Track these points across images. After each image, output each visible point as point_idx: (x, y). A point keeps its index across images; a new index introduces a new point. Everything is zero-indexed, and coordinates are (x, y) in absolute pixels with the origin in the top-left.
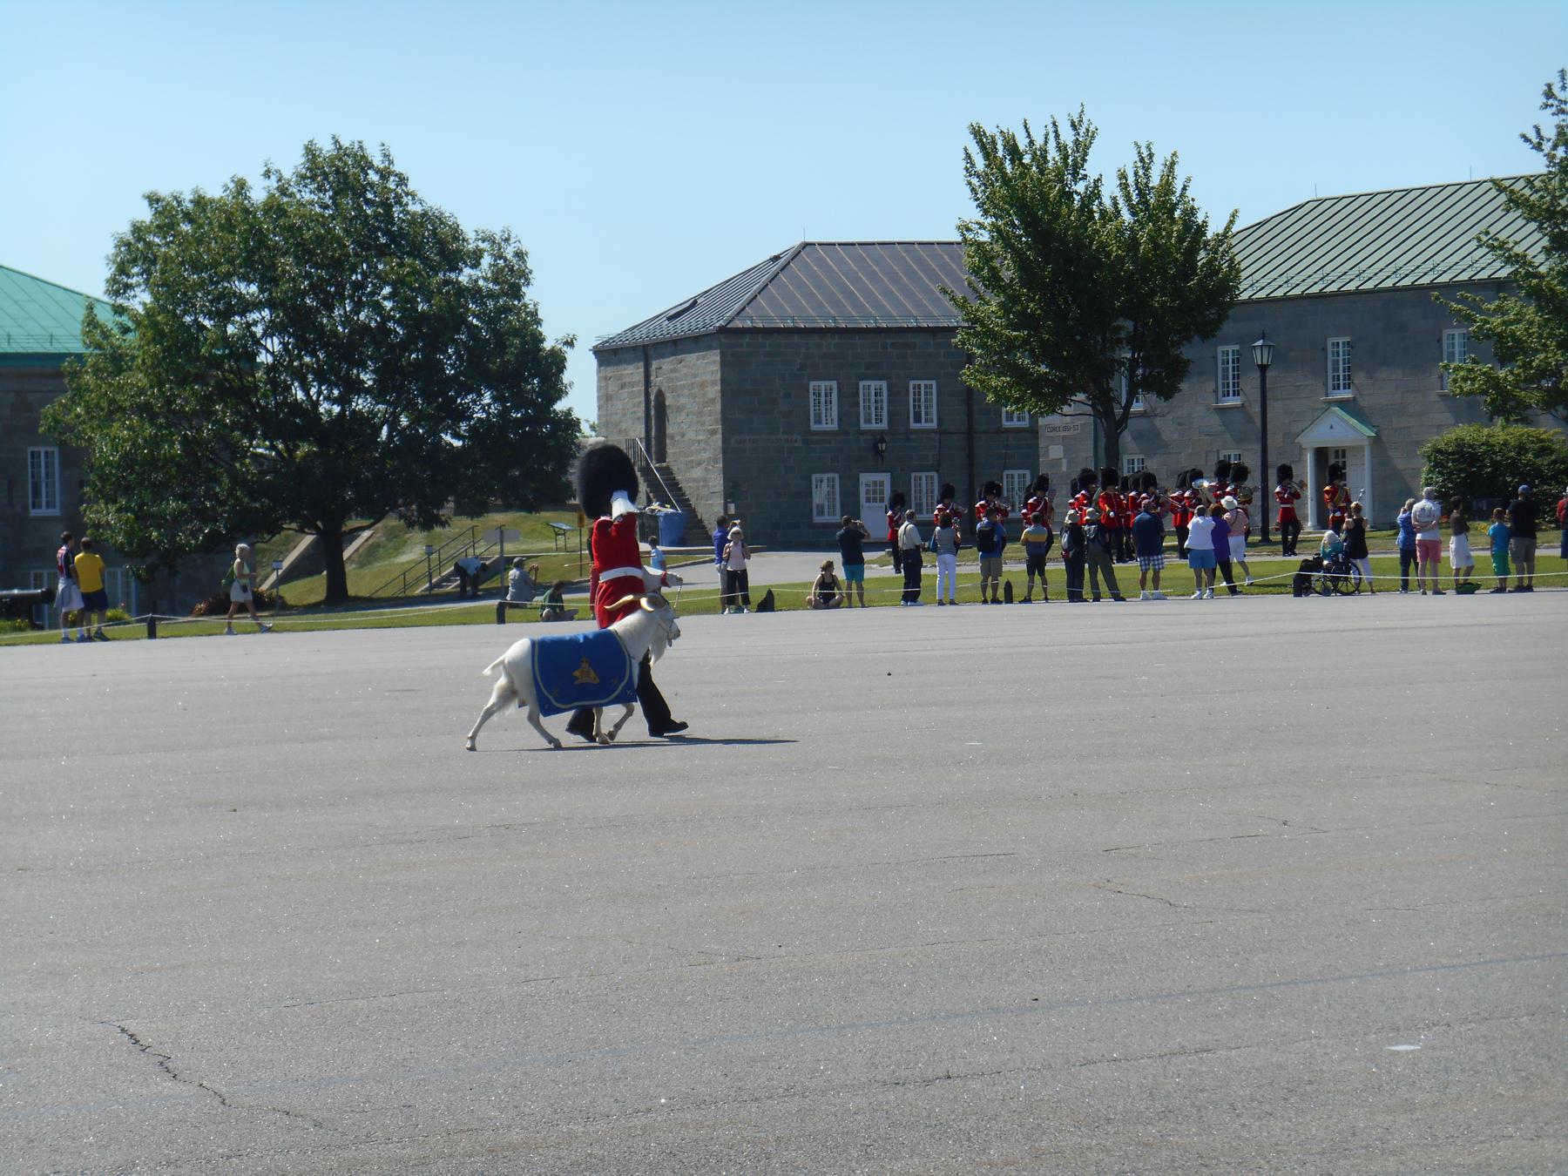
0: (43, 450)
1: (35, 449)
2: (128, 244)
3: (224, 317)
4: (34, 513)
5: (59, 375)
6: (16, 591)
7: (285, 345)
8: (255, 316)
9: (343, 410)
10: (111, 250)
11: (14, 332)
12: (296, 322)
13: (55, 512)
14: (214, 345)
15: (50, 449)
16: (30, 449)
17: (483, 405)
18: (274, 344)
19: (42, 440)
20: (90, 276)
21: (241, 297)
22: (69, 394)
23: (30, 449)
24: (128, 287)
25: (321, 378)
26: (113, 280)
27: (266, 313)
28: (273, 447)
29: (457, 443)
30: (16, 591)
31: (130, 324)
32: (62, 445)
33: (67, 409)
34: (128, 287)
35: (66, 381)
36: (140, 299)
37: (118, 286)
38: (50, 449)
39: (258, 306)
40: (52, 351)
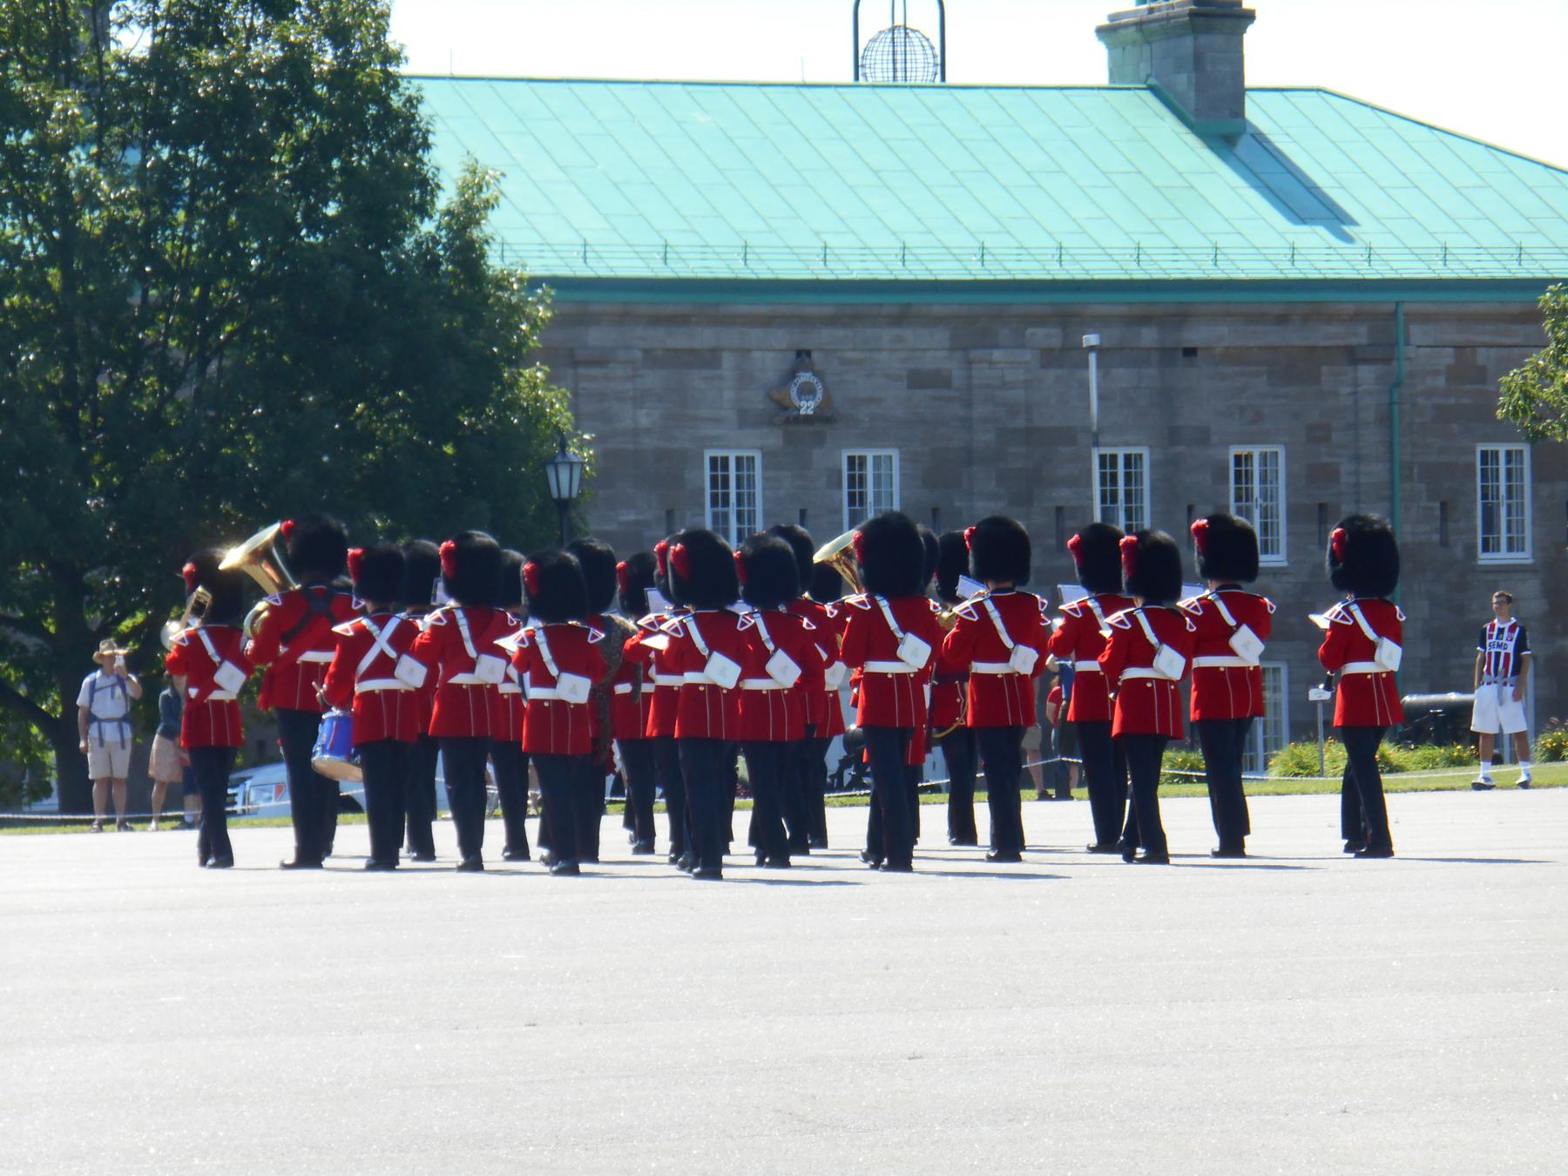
0: (1502, 449)
1: (1489, 447)
5: (1534, 317)
11: (1454, 241)
13: (1524, 557)
15: (1514, 447)
19: (1503, 432)
22: (1552, 349)
32: (1536, 438)
33: (1545, 377)
35: (1547, 325)
38: (1514, 447)
40: (1522, 274)
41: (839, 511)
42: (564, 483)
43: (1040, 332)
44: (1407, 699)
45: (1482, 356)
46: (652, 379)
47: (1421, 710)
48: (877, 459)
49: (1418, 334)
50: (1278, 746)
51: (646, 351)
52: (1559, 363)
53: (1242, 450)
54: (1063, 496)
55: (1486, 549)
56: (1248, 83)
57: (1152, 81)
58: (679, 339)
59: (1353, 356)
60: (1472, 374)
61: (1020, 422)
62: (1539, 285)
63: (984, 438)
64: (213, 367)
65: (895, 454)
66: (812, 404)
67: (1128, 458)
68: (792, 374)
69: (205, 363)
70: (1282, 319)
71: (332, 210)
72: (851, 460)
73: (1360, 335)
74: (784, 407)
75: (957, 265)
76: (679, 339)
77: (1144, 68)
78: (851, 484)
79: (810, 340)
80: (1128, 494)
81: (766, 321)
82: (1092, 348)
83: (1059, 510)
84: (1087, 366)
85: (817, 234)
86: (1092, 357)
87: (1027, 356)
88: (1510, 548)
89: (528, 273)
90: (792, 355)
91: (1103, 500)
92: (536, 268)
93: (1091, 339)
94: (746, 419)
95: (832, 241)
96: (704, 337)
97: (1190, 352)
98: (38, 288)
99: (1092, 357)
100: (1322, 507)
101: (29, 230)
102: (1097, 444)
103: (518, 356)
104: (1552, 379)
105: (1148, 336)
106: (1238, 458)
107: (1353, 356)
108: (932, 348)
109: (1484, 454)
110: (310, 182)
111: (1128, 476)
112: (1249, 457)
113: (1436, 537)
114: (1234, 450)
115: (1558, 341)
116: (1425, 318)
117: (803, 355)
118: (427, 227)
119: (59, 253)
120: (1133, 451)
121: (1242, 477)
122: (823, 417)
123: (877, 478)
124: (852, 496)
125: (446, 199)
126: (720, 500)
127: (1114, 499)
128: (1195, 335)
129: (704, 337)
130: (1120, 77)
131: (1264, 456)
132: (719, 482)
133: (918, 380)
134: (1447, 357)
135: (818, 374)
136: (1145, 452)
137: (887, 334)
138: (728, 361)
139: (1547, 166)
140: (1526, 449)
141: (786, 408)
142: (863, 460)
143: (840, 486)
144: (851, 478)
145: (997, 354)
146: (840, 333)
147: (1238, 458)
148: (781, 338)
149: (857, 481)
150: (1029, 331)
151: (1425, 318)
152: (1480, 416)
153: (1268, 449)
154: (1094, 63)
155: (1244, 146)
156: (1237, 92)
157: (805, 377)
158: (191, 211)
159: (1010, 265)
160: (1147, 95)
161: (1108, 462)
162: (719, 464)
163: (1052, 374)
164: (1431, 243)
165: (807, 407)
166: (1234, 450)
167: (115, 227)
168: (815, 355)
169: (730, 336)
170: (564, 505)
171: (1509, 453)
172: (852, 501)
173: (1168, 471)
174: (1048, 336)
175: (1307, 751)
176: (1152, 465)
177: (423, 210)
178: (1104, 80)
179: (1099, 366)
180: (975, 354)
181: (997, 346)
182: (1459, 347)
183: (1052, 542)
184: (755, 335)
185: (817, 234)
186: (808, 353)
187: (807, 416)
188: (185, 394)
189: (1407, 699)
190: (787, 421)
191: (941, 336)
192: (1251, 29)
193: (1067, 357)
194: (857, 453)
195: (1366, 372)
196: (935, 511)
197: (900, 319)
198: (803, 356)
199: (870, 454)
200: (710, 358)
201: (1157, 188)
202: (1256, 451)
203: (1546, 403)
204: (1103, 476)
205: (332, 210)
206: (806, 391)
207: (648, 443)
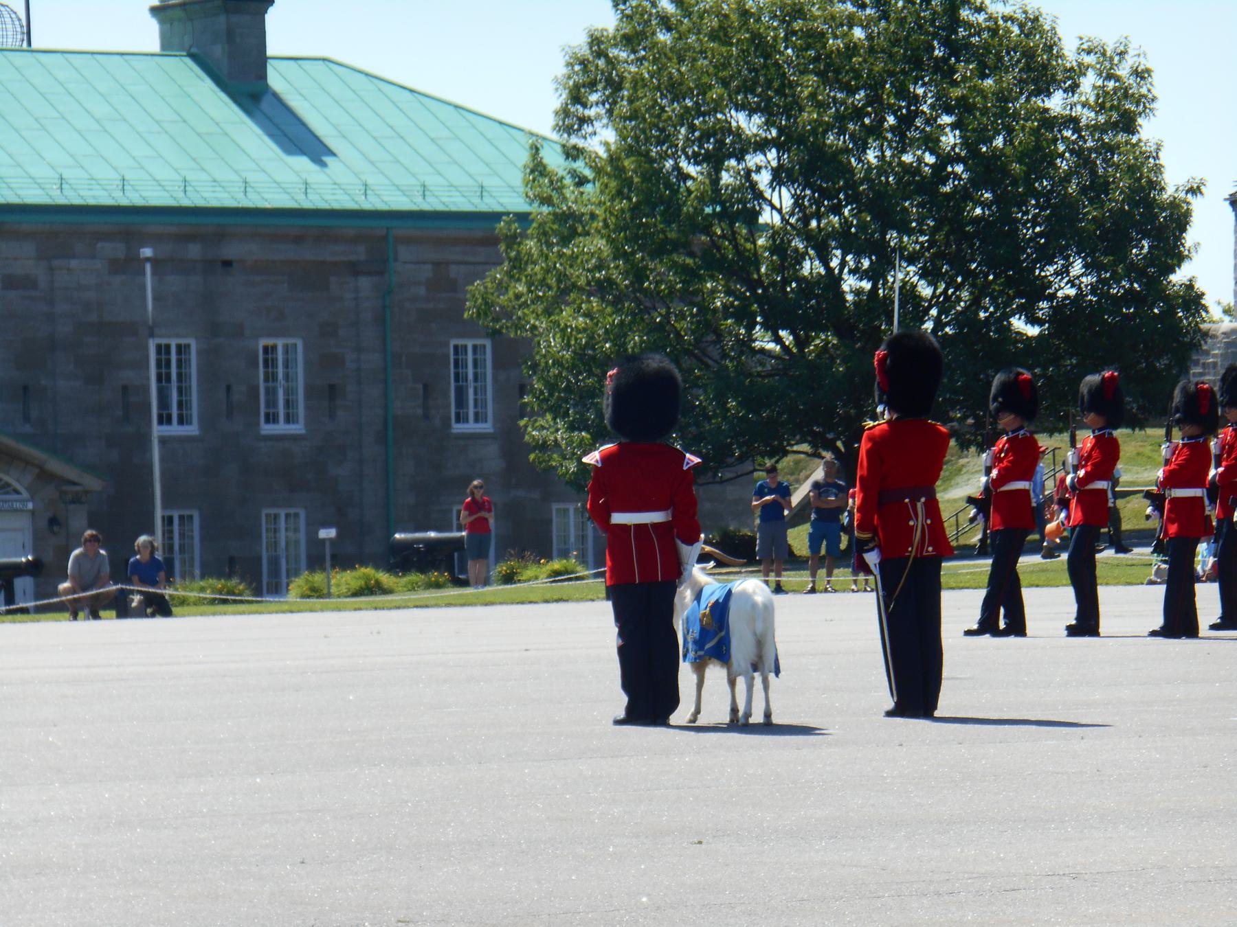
0: (470, 344)
1: (460, 342)
2: (584, 63)
3: (715, 161)
4: (458, 428)
6: (432, 534)
7: (798, 200)
8: (753, 160)
9: (875, 289)
10: (562, 71)
11: (432, 181)
12: (813, 167)
13: (487, 427)
14: (702, 199)
15: (479, 342)
16: (453, 342)
17: (1071, 279)
18: (785, 198)
19: (469, 329)
20: (538, 108)
21: (738, 133)
23: (453, 342)
24: (583, 120)
25: (848, 242)
26: (565, 112)
27: (772, 154)
28: (778, 340)
29: (1033, 331)
30: (432, 534)
31: (588, 173)
32: (495, 334)
33: (502, 288)
34: (583, 120)
35: (502, 247)
36: (602, 138)
37: (572, 120)
38: (479, 342)
39: (761, 146)
44: (397, 536)
45: (454, 271)
47: (407, 546)
49: (405, 253)
50: (297, 573)
52: (512, 277)
53: (269, 342)
54: (127, 376)
55: (458, 420)
56: (270, 52)
57: (194, 50)
59: (354, 269)
60: (446, 285)
62: (495, 216)
67: (179, 347)
70: (298, 240)
73: (360, 253)
75: (40, 192)
77: (188, 40)
80: (180, 376)
82: (147, 259)
84: (144, 273)
86: (148, 267)
88: (476, 420)
91: (159, 379)
93: (147, 252)
97: (227, 264)
99: (148, 268)
100: (332, 387)
102: (152, 335)
104: (507, 289)
105: (194, 251)
106: (266, 349)
107: (354, 269)
109: (456, 347)
111: (179, 362)
112: (274, 348)
113: (420, 411)
114: (263, 342)
115: (510, 260)
116: (408, 241)
120: (183, 341)
121: (270, 363)
127: (169, 380)
128: (231, 251)
130: (168, 44)
131: (286, 349)
134: (427, 271)
136: (193, 343)
139: (501, 123)
140: (488, 344)
145: (74, 263)
147: (266, 349)
150: (99, 245)
151: (408, 241)
152: (452, 318)
153: (290, 341)
154: (148, 35)
155: (265, 104)
156: (261, 59)
159: (82, 193)
160: (188, 61)
161: (163, 350)
164: (415, 182)
166: (263, 342)
171: (475, 347)
174: (113, 249)
175: (318, 578)
176: (199, 353)
178: (155, 46)
179: (154, 273)
180: (56, 263)
181: (74, 257)
182: (437, 264)
189: (397, 536)
191: (29, 248)
192: (271, 10)
193: (131, 265)
195: (364, 282)
202: (280, 343)
203: (502, 307)
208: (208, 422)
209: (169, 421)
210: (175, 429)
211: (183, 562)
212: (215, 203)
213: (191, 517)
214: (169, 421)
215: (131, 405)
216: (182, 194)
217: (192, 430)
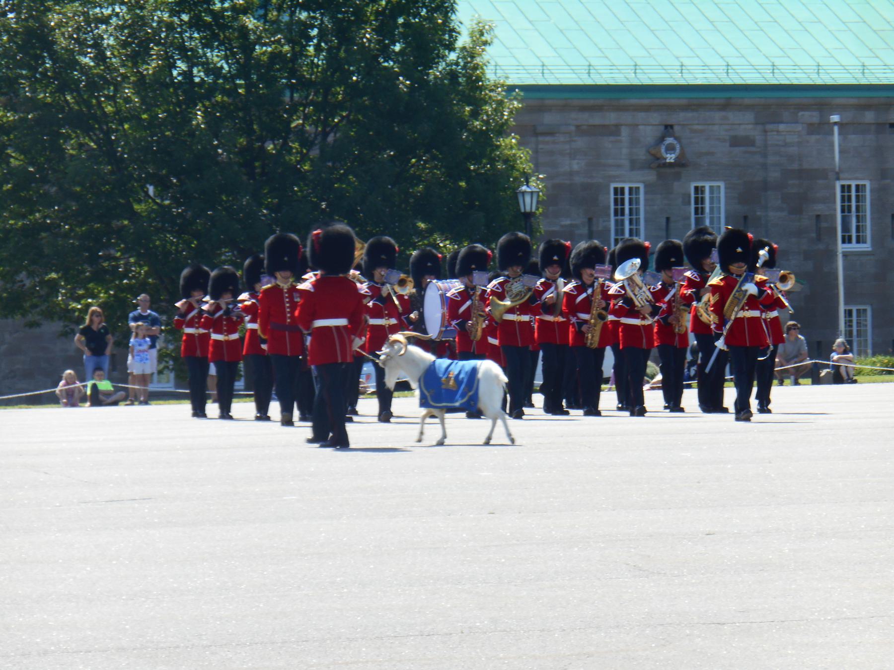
41: (689, 218)
42: (528, 204)
43: (807, 114)
46: (581, 142)
48: (711, 188)
51: (578, 127)
54: (819, 208)
58: (597, 119)
61: (795, 166)
63: (774, 175)
64: (331, 138)
65: (722, 185)
66: (673, 156)
67: (857, 186)
68: (662, 139)
69: (325, 134)
71: (397, 47)
72: (696, 188)
74: (657, 158)
75: (758, 75)
76: (597, 119)
78: (696, 203)
79: (672, 119)
80: (858, 207)
81: (647, 109)
82: (835, 123)
83: (818, 216)
84: (832, 133)
85: (677, 58)
86: (836, 129)
87: (799, 128)
89: (510, 82)
90: (662, 128)
91: (843, 211)
92: (513, 80)
93: (835, 118)
94: (634, 165)
95: (686, 62)
96: (611, 118)
98: (232, 92)
99: (836, 129)
101: (226, 58)
102: (838, 179)
103: (502, 130)
105: (869, 117)
108: (744, 123)
110: (385, 30)
111: (857, 197)
117: (668, 128)
118: (453, 56)
119: (243, 71)
122: (680, 164)
123: (712, 202)
124: (696, 209)
125: (463, 40)
126: (619, 212)
127: (850, 211)
129: (611, 118)
132: (619, 202)
133: (736, 142)
135: (676, 138)
137: (718, 115)
138: (625, 132)
141: (658, 159)
142: (703, 187)
143: (689, 203)
144: (696, 199)
145: (782, 127)
146: (690, 115)
148: (656, 118)
149: (699, 201)
150: (801, 113)
157: (670, 140)
158: (318, 48)
159: (788, 76)
161: (846, 189)
162: (619, 191)
163: (813, 138)
165: (671, 158)
167: (275, 57)
168: (676, 128)
169: (627, 118)
170: (528, 216)
172: (696, 213)
173: (880, 193)
176: (871, 191)
177: (451, 47)
179: (840, 134)
180: (769, 127)
181: (782, 122)
183: (814, 235)
184: (642, 115)
185: (677, 58)
186: (672, 126)
187: (671, 165)
188: (315, 153)
190: (659, 166)
191: (749, 116)
193: (823, 128)
194: (699, 184)
196: (745, 218)
197: (726, 106)
198: (668, 128)
199: (707, 185)
200: (614, 130)
201: (875, 31)
204: (843, 197)
205: (397, 47)
206: (670, 149)
207: (578, 180)
208: (878, 241)
209: (850, 241)
210: (854, 247)
211: (859, 345)
212: (885, 82)
213: (865, 310)
214: (850, 241)
215: (822, 230)
216: (860, 76)
217: (866, 247)
